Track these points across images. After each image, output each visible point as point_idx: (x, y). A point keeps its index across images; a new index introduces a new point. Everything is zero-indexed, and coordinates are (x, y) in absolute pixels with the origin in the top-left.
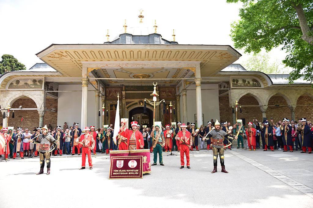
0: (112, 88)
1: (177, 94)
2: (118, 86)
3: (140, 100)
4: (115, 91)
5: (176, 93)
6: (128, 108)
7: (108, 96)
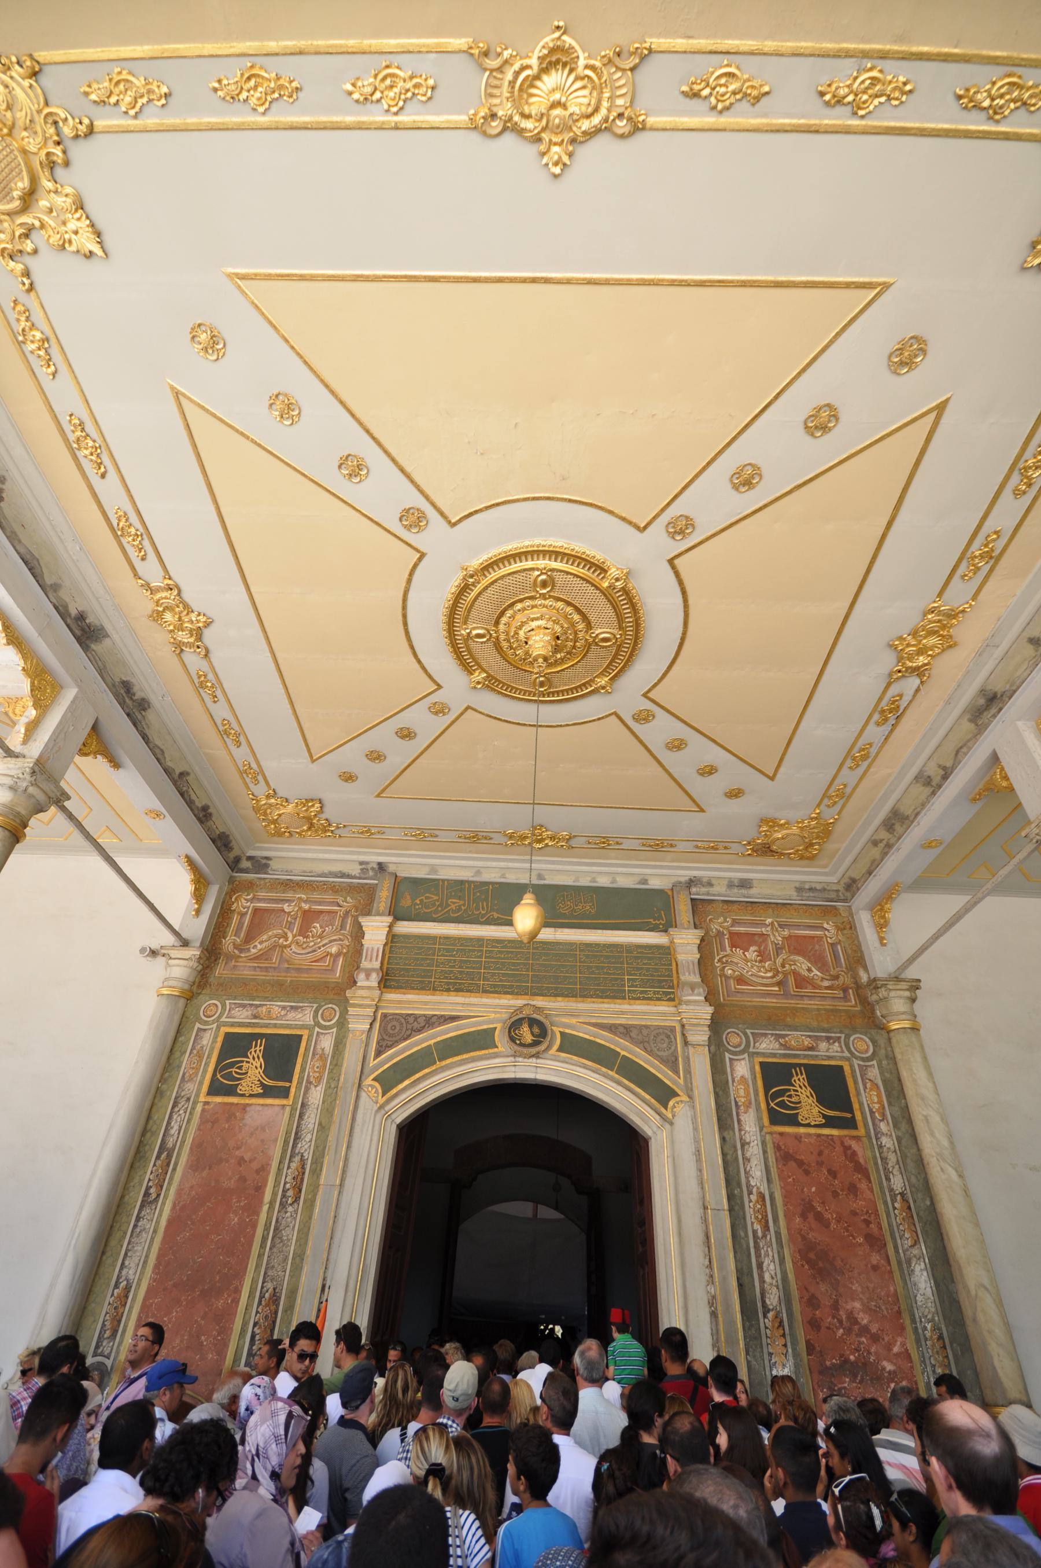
0: (289, 895)
1: (881, 962)
2: (343, 875)
4: (308, 917)
5: (858, 959)
6: (388, 1081)
7: (229, 957)
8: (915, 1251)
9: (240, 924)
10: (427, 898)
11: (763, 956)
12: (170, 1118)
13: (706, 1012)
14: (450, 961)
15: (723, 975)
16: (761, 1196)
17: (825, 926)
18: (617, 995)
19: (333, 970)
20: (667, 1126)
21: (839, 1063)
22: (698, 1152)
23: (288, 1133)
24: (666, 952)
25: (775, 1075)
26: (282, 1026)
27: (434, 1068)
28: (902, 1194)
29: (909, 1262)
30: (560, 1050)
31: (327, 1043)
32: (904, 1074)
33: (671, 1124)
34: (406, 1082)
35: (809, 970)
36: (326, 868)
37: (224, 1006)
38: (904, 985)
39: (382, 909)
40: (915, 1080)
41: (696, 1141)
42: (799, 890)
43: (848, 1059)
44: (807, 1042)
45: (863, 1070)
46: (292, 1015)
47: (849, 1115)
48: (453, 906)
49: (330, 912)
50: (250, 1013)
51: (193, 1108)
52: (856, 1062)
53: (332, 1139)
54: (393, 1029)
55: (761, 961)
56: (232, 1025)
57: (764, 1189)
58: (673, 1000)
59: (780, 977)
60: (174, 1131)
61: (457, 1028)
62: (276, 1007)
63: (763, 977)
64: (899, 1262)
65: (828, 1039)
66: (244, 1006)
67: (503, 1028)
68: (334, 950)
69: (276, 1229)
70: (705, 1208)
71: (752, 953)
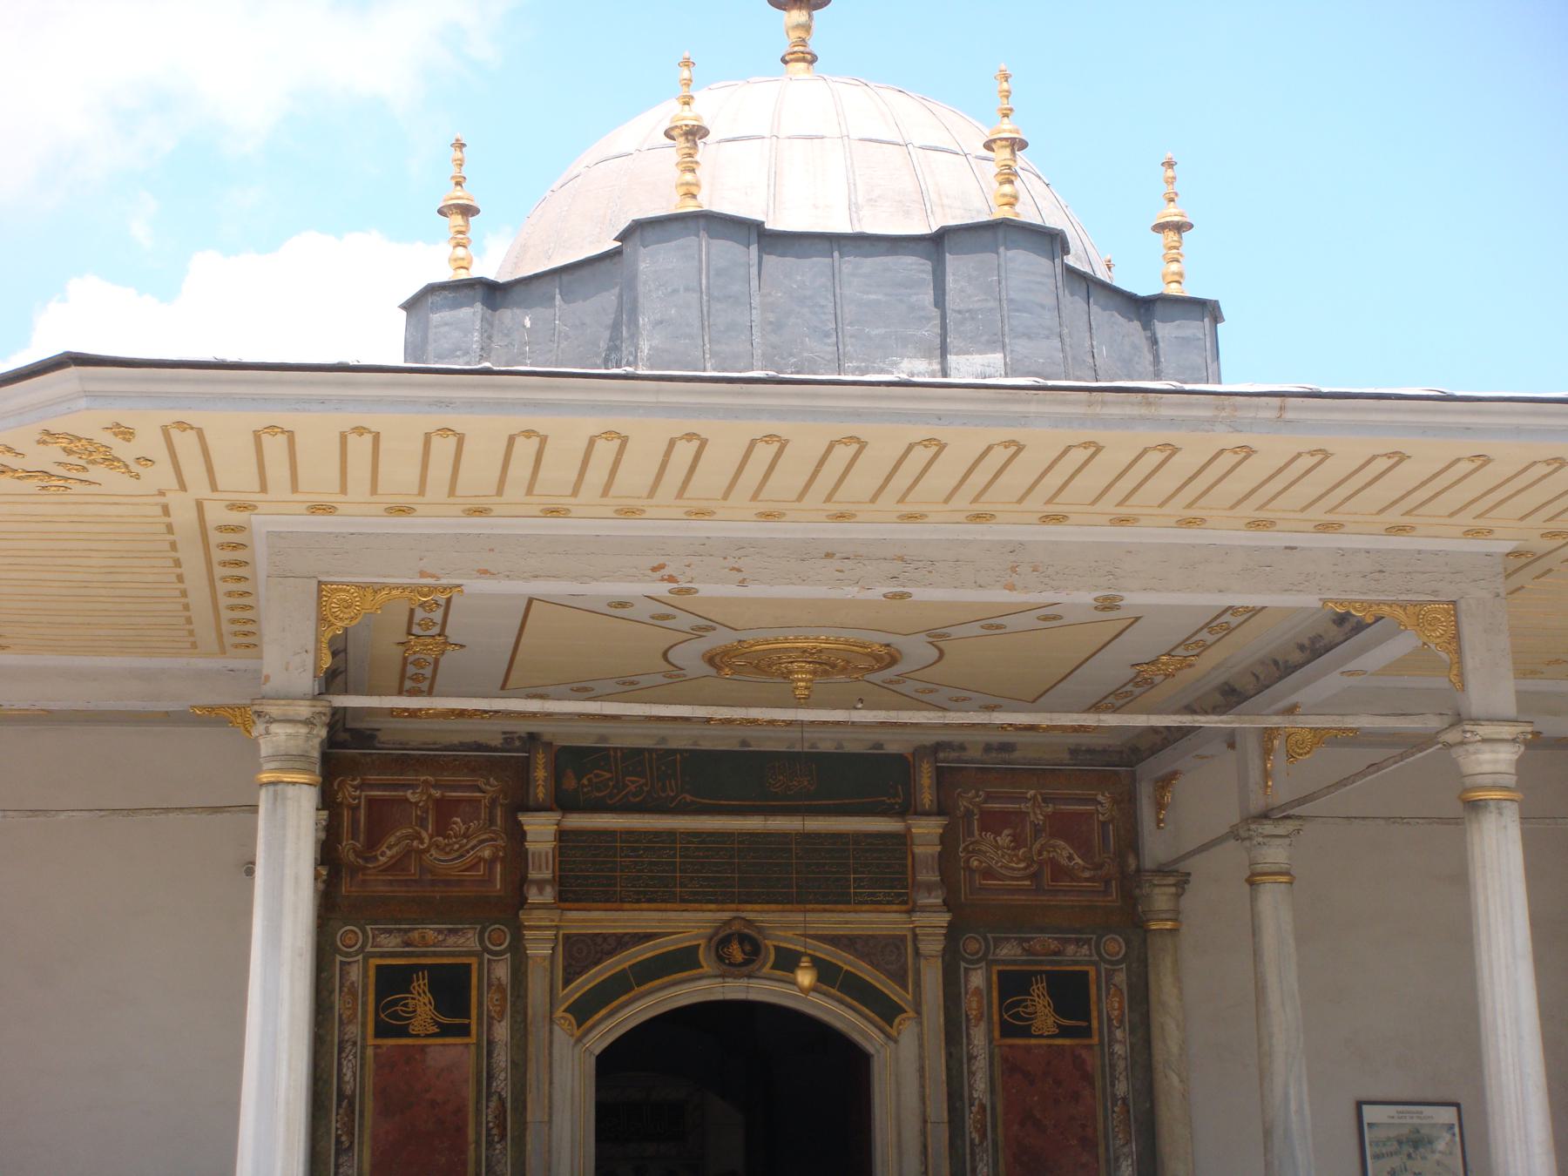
0: (409, 777)
1: (1156, 847)
2: (479, 747)
3: (726, 916)
4: (444, 810)
5: (1131, 842)
6: (583, 1011)
8: (1125, 1150)
9: (355, 821)
10: (597, 776)
11: (1018, 841)
12: (340, 1064)
13: (944, 919)
14: (636, 863)
15: (968, 868)
16: (983, 1107)
17: (1100, 798)
18: (835, 896)
19: (490, 880)
20: (891, 1044)
21: (1085, 968)
22: (922, 1069)
23: (479, 1073)
24: (902, 841)
25: (1012, 984)
26: (442, 954)
27: (631, 994)
28: (1124, 1099)
29: (1117, 1159)
30: (773, 968)
31: (502, 972)
32: (1152, 978)
33: (896, 1041)
34: (603, 1012)
35: (1070, 858)
36: (456, 740)
37: (364, 932)
38: (1171, 880)
39: (541, 795)
40: (1165, 987)
41: (921, 1058)
42: (1074, 751)
43: (1095, 964)
44: (1053, 946)
45: (1110, 974)
46: (451, 940)
47: (1084, 1024)
48: (632, 787)
49: (470, 801)
50: (399, 940)
51: (363, 1053)
52: (1103, 966)
53: (531, 1075)
54: (579, 953)
55: (1014, 849)
56: (382, 955)
57: (986, 1101)
58: (905, 903)
59: (1035, 867)
60: (348, 1077)
61: (654, 947)
62: (430, 931)
63: (1014, 869)
64: (1108, 1161)
65: (1077, 941)
66: (390, 932)
67: (708, 947)
68: (487, 853)
69: (487, 1166)
70: (925, 1122)
71: (1004, 839)
